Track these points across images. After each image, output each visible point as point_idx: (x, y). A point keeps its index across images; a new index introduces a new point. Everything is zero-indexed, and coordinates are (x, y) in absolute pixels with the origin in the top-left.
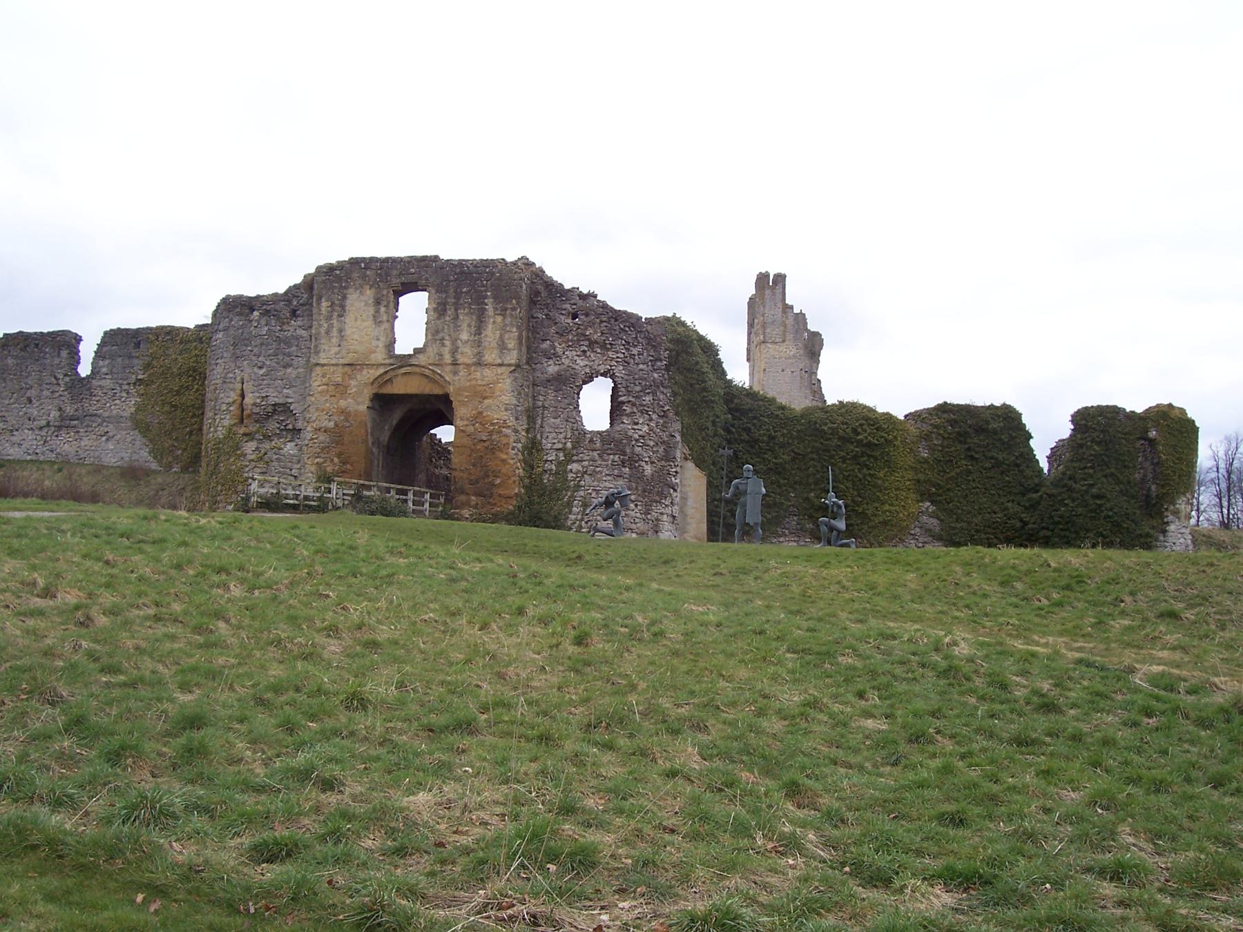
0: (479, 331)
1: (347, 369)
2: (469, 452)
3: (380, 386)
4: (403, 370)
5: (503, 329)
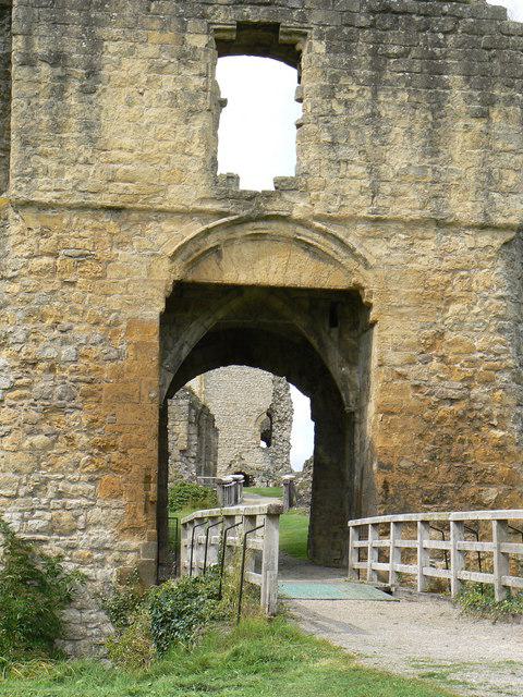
0: (433, 147)
1: (108, 222)
2: (420, 426)
3: (194, 263)
4: (249, 229)
5: (485, 143)
